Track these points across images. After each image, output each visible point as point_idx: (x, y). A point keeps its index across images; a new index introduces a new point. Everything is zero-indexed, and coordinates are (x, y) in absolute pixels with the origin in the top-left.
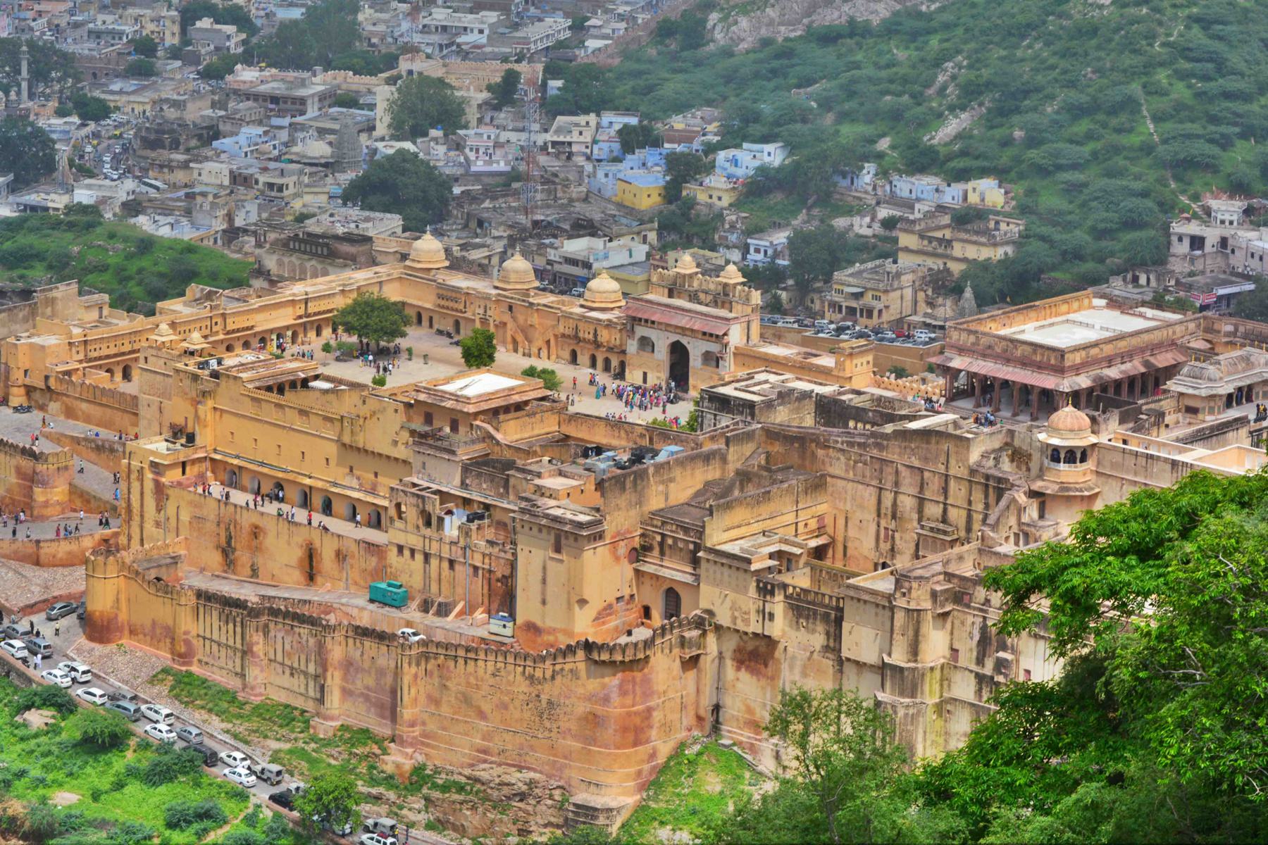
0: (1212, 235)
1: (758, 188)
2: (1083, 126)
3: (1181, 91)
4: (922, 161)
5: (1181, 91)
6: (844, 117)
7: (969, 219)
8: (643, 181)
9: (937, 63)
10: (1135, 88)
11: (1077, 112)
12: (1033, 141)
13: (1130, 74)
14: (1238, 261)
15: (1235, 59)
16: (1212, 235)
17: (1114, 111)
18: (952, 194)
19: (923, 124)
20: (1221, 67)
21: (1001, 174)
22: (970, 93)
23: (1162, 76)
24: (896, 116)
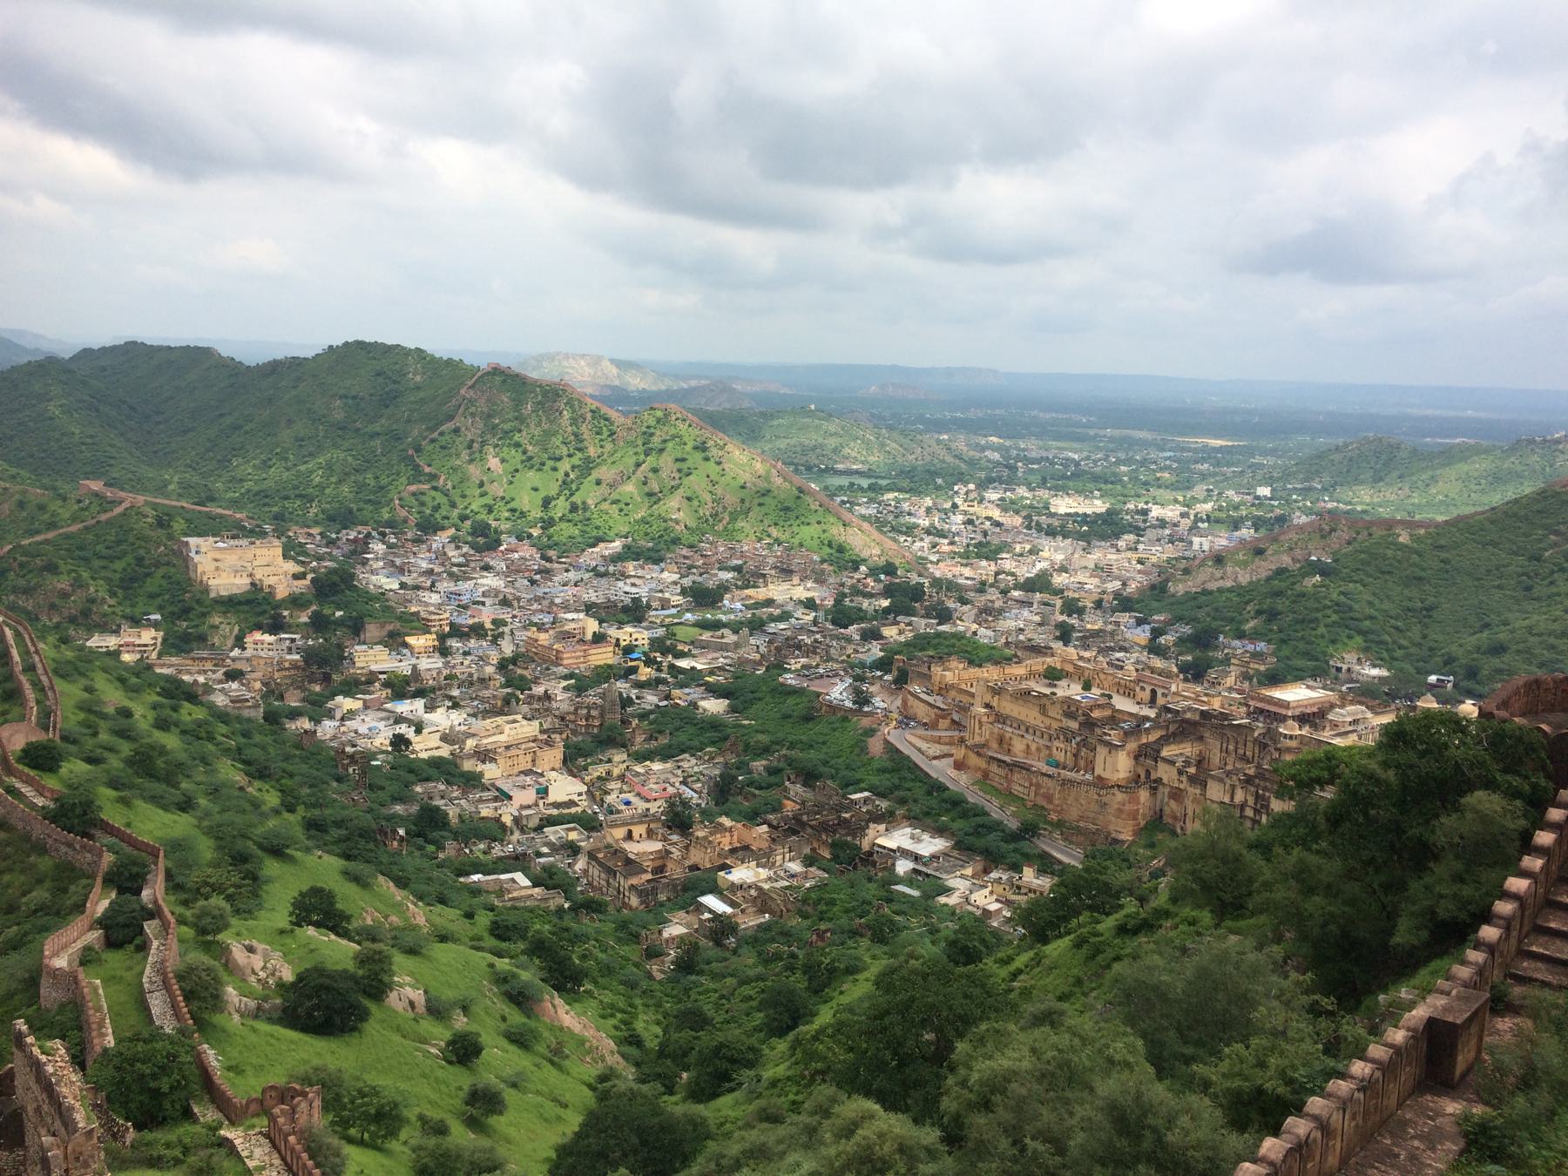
0: (1345, 667)
1: (1181, 641)
2: (1298, 627)
3: (1335, 617)
4: (1241, 636)
5: (1335, 617)
6: (1214, 619)
7: (1256, 656)
8: (1142, 635)
9: (1247, 603)
10: (1319, 615)
11: (1297, 622)
12: (1280, 631)
13: (1317, 610)
14: (1354, 676)
15: (1356, 607)
16: (1345, 667)
17: (1311, 621)
18: (1250, 647)
19: (1240, 623)
20: (1351, 609)
21: (1269, 642)
22: (1259, 613)
23: (1329, 612)
24: (1232, 620)
